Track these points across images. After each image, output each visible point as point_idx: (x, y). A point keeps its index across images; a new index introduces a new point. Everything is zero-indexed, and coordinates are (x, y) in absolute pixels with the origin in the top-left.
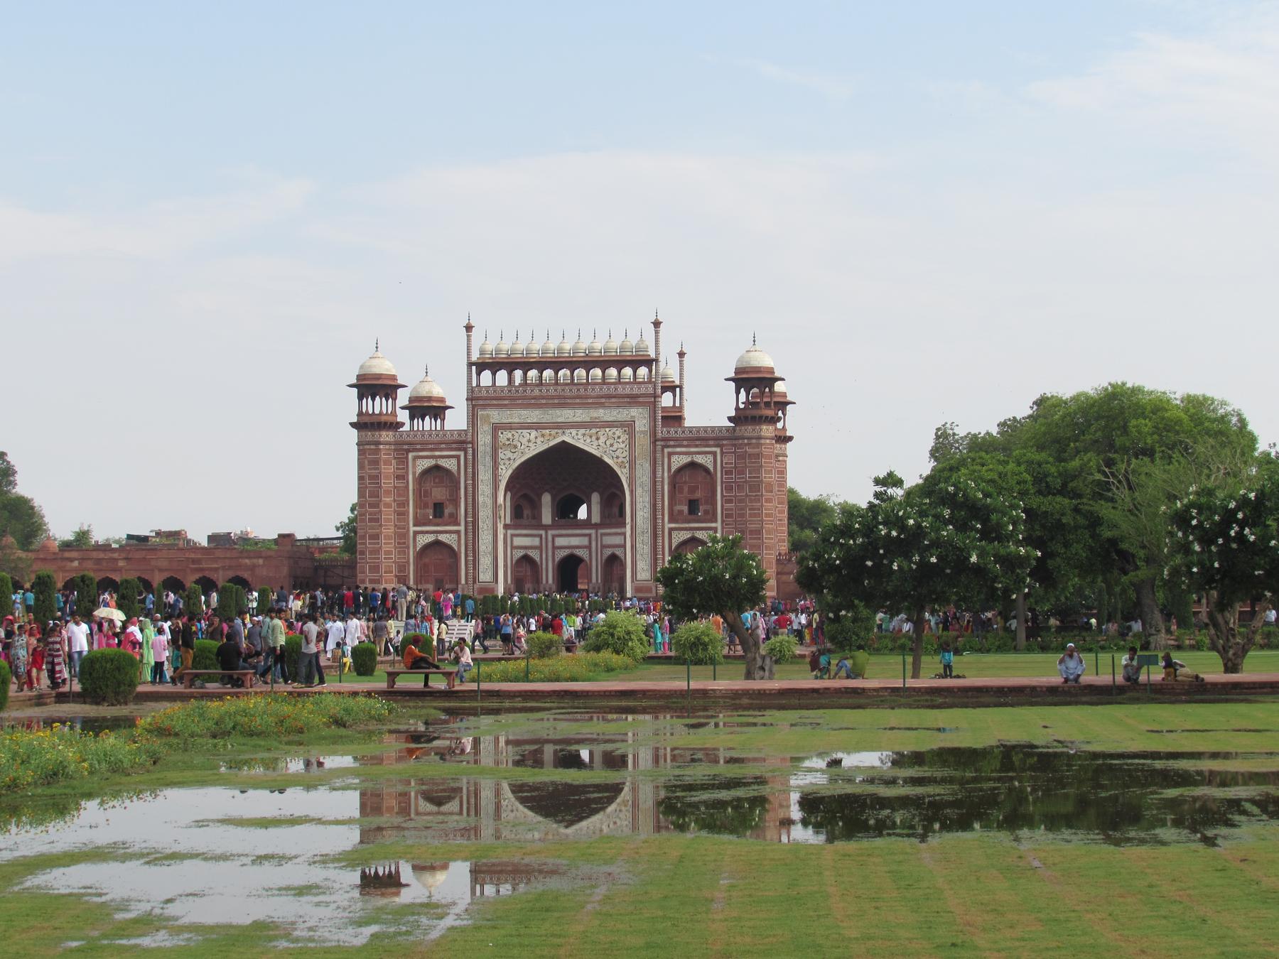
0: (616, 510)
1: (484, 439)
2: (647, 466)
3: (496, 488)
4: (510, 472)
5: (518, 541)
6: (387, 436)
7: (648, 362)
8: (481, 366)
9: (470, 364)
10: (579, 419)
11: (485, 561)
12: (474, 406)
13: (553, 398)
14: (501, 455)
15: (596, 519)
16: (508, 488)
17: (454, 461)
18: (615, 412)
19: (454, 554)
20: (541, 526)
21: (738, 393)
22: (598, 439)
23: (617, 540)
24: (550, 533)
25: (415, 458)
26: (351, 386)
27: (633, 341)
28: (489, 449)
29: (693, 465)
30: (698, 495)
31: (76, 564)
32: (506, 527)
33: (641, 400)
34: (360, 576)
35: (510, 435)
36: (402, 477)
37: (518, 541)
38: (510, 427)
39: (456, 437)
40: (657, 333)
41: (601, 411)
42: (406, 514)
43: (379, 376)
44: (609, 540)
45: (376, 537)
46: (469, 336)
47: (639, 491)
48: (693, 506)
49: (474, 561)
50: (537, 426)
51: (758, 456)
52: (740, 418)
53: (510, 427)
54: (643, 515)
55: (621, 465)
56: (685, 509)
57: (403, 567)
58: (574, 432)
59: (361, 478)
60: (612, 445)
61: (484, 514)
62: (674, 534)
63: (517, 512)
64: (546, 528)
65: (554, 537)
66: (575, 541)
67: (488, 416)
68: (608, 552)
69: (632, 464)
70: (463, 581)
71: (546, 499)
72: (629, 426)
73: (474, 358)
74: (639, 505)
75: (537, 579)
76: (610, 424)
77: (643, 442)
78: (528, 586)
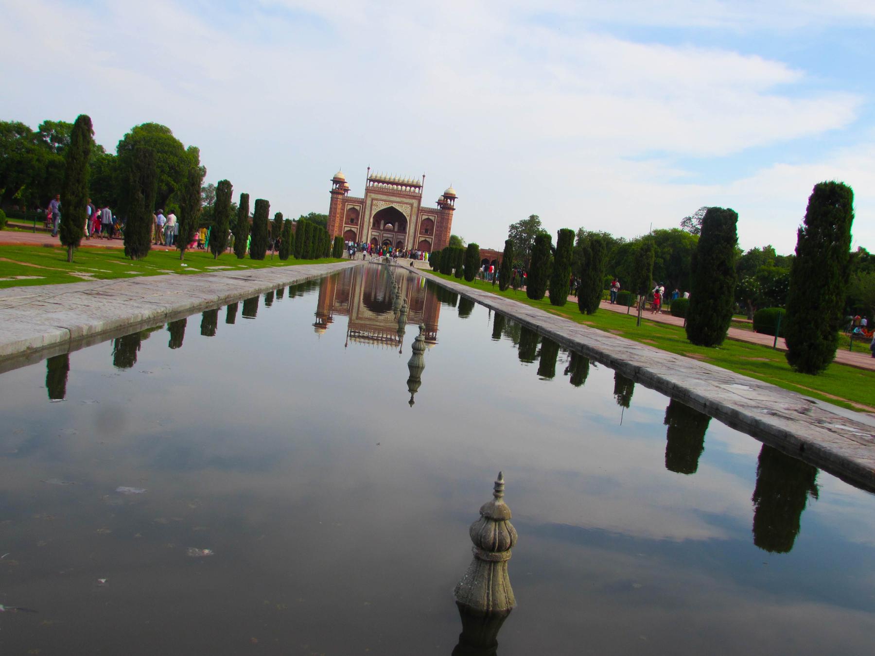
1: (369, 202)
6: (340, 197)
7: (419, 187)
8: (371, 180)
15: (396, 229)
19: (355, 234)
29: (428, 219)
36: (343, 210)
38: (377, 200)
48: (426, 231)
53: (377, 200)
63: (374, 225)
71: (382, 222)
72: (412, 205)
74: (411, 228)
76: (407, 203)
77: (415, 210)
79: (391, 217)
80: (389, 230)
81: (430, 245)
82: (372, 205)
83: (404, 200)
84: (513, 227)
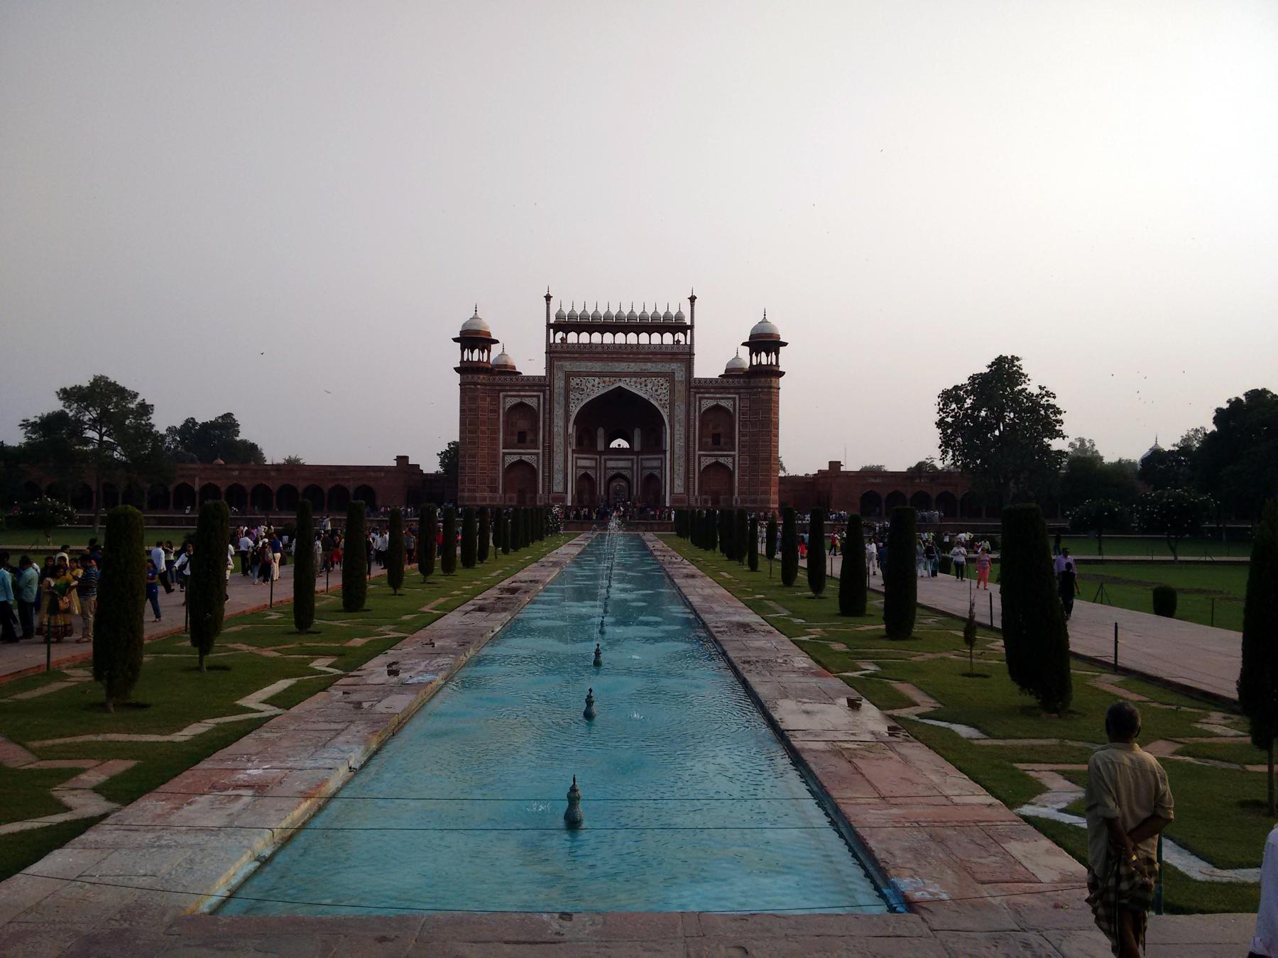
1: (559, 384)
3: (567, 421)
5: (582, 463)
6: (482, 378)
9: (549, 326)
11: (558, 477)
13: (612, 353)
15: (637, 447)
16: (575, 423)
17: (535, 399)
18: (660, 365)
19: (534, 472)
23: (656, 463)
25: (505, 397)
26: (455, 340)
27: (674, 312)
29: (717, 408)
30: (720, 430)
31: (236, 473)
32: (573, 451)
34: (460, 486)
37: (582, 463)
38: (578, 374)
40: (692, 306)
42: (496, 439)
43: (478, 332)
44: (647, 464)
45: (473, 456)
47: (677, 426)
48: (716, 439)
50: (600, 375)
51: (770, 401)
53: (578, 374)
54: (680, 443)
55: (664, 406)
56: (710, 440)
57: (494, 480)
59: (462, 411)
61: (558, 441)
62: (703, 459)
64: (601, 453)
66: (621, 464)
68: (647, 472)
69: (672, 404)
71: (601, 432)
72: (670, 377)
73: (552, 320)
74: (675, 437)
75: (593, 491)
76: (657, 375)
77: (680, 388)
78: (586, 496)
79: (618, 413)
80: (620, 451)
81: (731, 474)
83: (650, 367)
84: (950, 396)
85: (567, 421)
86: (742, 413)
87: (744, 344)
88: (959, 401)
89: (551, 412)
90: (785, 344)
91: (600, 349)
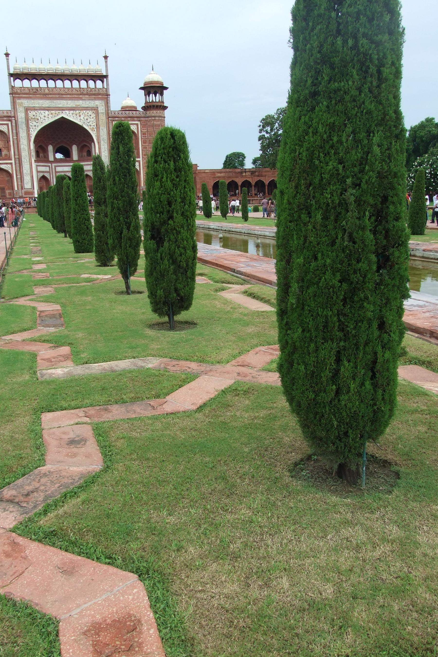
0: (85, 154)
1: (21, 115)
2: (105, 130)
3: (29, 141)
4: (36, 132)
5: (40, 169)
10: (70, 106)
11: (27, 178)
12: (14, 97)
14: (30, 124)
19: (10, 175)
20: (48, 161)
21: (145, 95)
22: (80, 116)
24: (54, 165)
28: (24, 120)
33: (100, 96)
35: (34, 114)
37: (41, 169)
38: (34, 109)
39: (5, 114)
40: (106, 62)
41: (81, 102)
46: (7, 59)
47: (102, 143)
49: (21, 178)
52: (147, 107)
53: (34, 109)
58: (67, 112)
60: (87, 119)
61: (25, 154)
64: (51, 162)
65: (55, 167)
67: (22, 103)
70: (16, 189)
71: (50, 148)
72: (95, 109)
73: (11, 72)
76: (86, 109)
77: (103, 118)
82: (27, 120)
85: (29, 141)
86: (143, 134)
87: (141, 88)
88: (272, 124)
89: (17, 134)
90: (166, 88)
91: (47, 91)
